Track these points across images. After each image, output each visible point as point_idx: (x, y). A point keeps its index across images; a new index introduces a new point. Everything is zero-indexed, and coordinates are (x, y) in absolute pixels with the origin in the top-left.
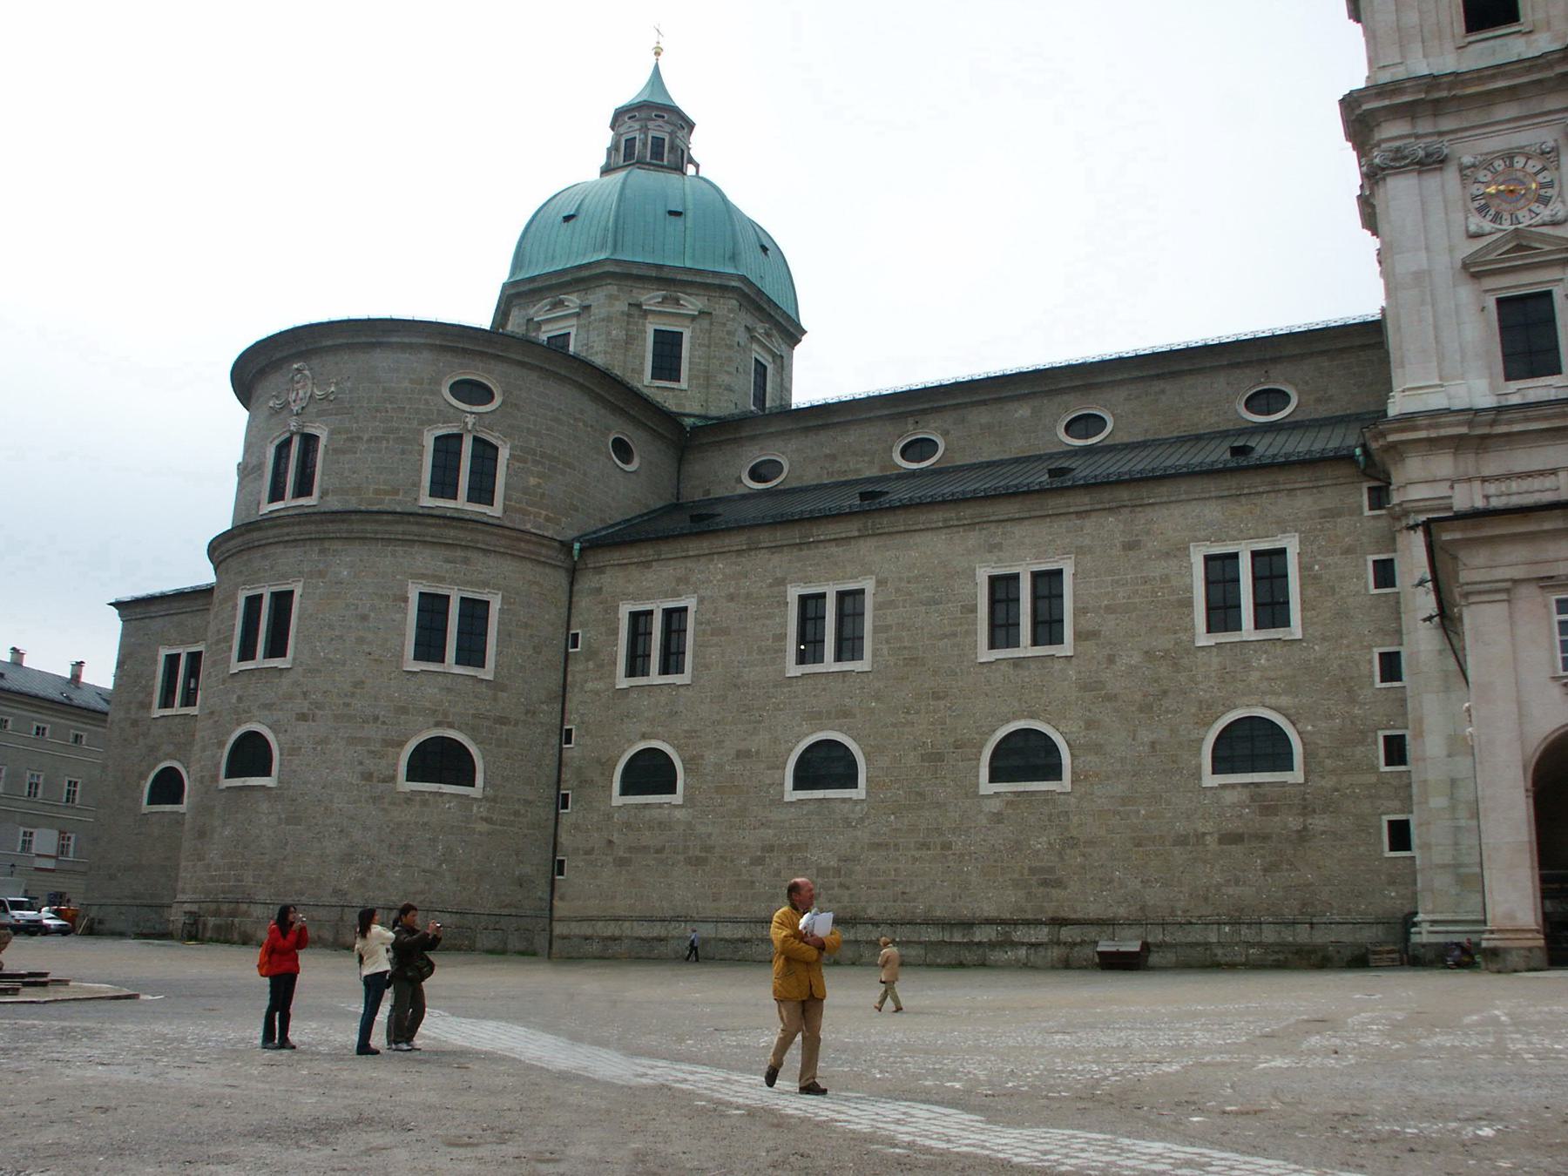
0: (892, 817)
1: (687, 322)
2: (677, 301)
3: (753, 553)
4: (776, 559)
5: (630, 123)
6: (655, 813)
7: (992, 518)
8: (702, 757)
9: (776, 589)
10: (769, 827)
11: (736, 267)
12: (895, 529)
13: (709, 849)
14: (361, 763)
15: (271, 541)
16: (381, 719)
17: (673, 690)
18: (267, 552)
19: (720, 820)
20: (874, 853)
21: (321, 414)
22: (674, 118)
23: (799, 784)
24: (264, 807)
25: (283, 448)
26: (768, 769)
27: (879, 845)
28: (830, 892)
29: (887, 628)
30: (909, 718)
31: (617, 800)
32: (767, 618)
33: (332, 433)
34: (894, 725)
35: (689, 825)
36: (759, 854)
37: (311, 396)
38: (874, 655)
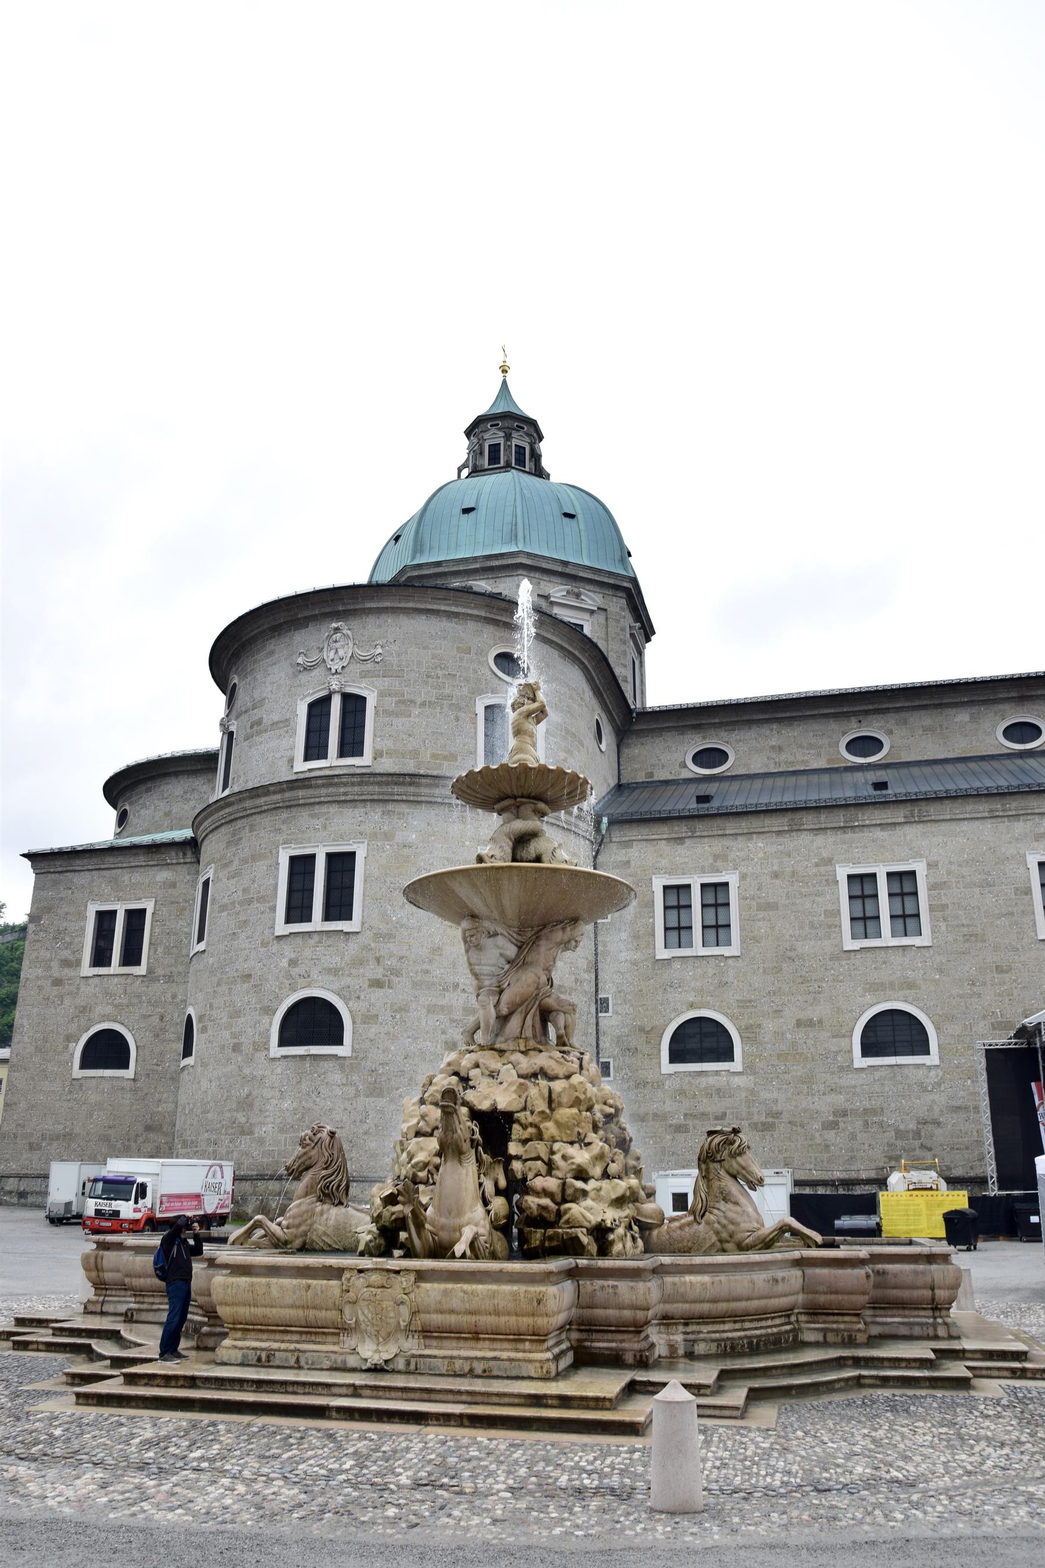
0: (969, 1081)
1: (587, 616)
2: (578, 596)
3: (794, 834)
4: (820, 840)
5: (494, 430)
6: (712, 1080)
7: (1037, 811)
8: (759, 1026)
9: (822, 869)
10: (840, 1093)
11: (625, 569)
12: (942, 817)
13: (778, 1114)
14: (444, 1032)
15: (322, 799)
16: (461, 987)
17: (720, 961)
18: (316, 811)
19: (785, 1086)
20: (955, 1116)
21: (364, 675)
22: (532, 431)
23: (867, 1050)
24: (337, 1077)
25: (319, 709)
26: (833, 1037)
27: (959, 1108)
28: (912, 1154)
29: (944, 907)
30: (975, 989)
31: (667, 1067)
32: (818, 894)
33: (381, 695)
34: (961, 996)
35: (752, 1092)
36: (831, 1118)
37: (352, 656)
38: (933, 932)
